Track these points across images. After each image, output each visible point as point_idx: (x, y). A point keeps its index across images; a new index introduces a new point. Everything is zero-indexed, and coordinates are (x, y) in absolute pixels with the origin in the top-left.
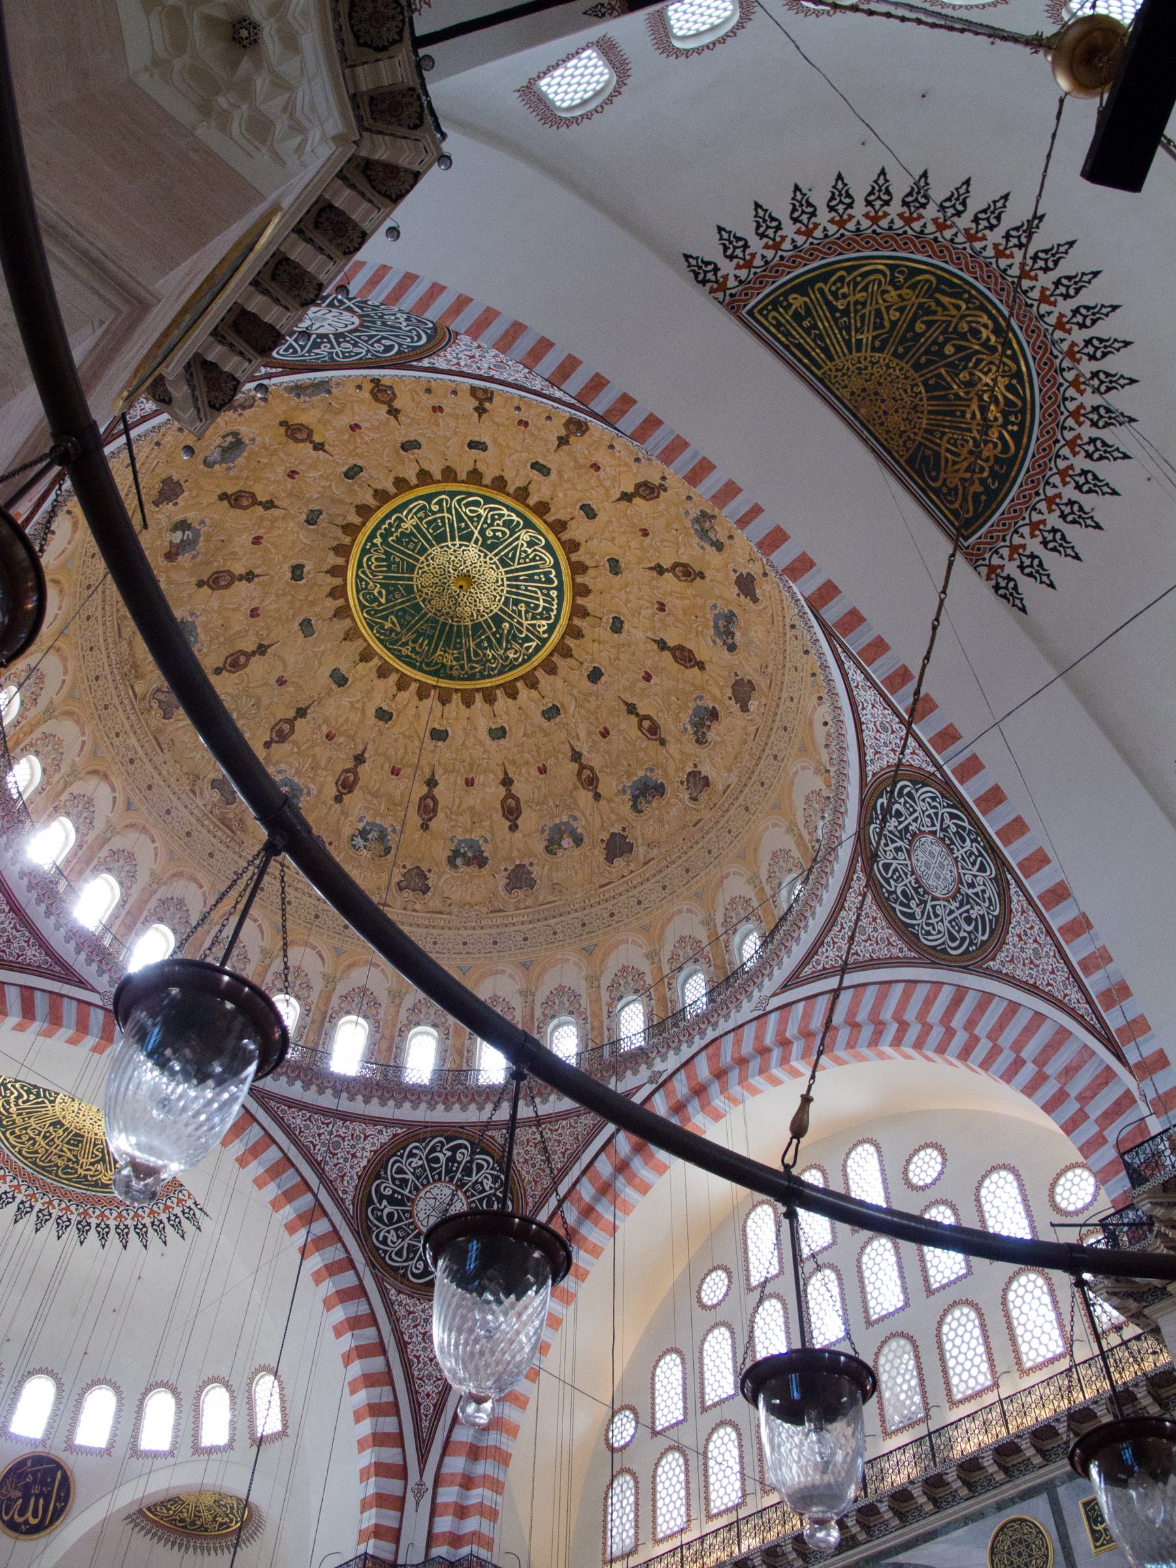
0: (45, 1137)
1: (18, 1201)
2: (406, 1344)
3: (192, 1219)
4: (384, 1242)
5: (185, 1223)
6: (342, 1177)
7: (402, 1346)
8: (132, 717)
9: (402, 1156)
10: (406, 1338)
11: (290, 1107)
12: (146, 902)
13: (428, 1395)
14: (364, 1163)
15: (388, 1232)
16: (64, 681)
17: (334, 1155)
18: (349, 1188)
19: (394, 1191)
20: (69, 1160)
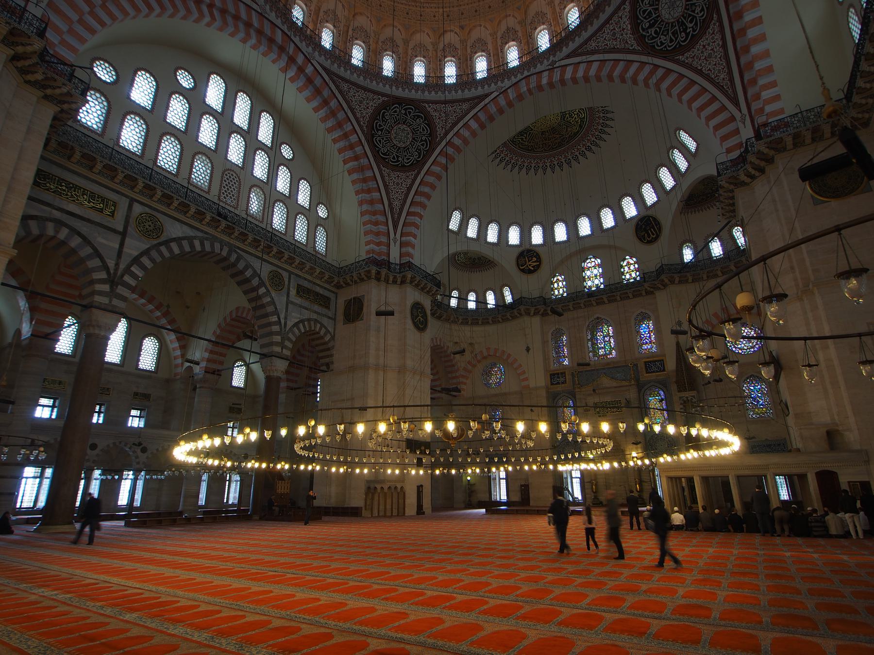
0: (546, 140)
1: (556, 164)
2: (701, 70)
3: (608, 112)
4: (662, 44)
5: (607, 115)
6: (627, 42)
7: (699, 72)
8: (432, 5)
9: (640, 6)
10: (699, 68)
11: (586, 44)
12: (497, 44)
13: (723, 79)
14: (629, 26)
15: (660, 38)
16: (399, 29)
17: (616, 39)
18: (633, 43)
19: (649, 22)
20: (560, 137)
